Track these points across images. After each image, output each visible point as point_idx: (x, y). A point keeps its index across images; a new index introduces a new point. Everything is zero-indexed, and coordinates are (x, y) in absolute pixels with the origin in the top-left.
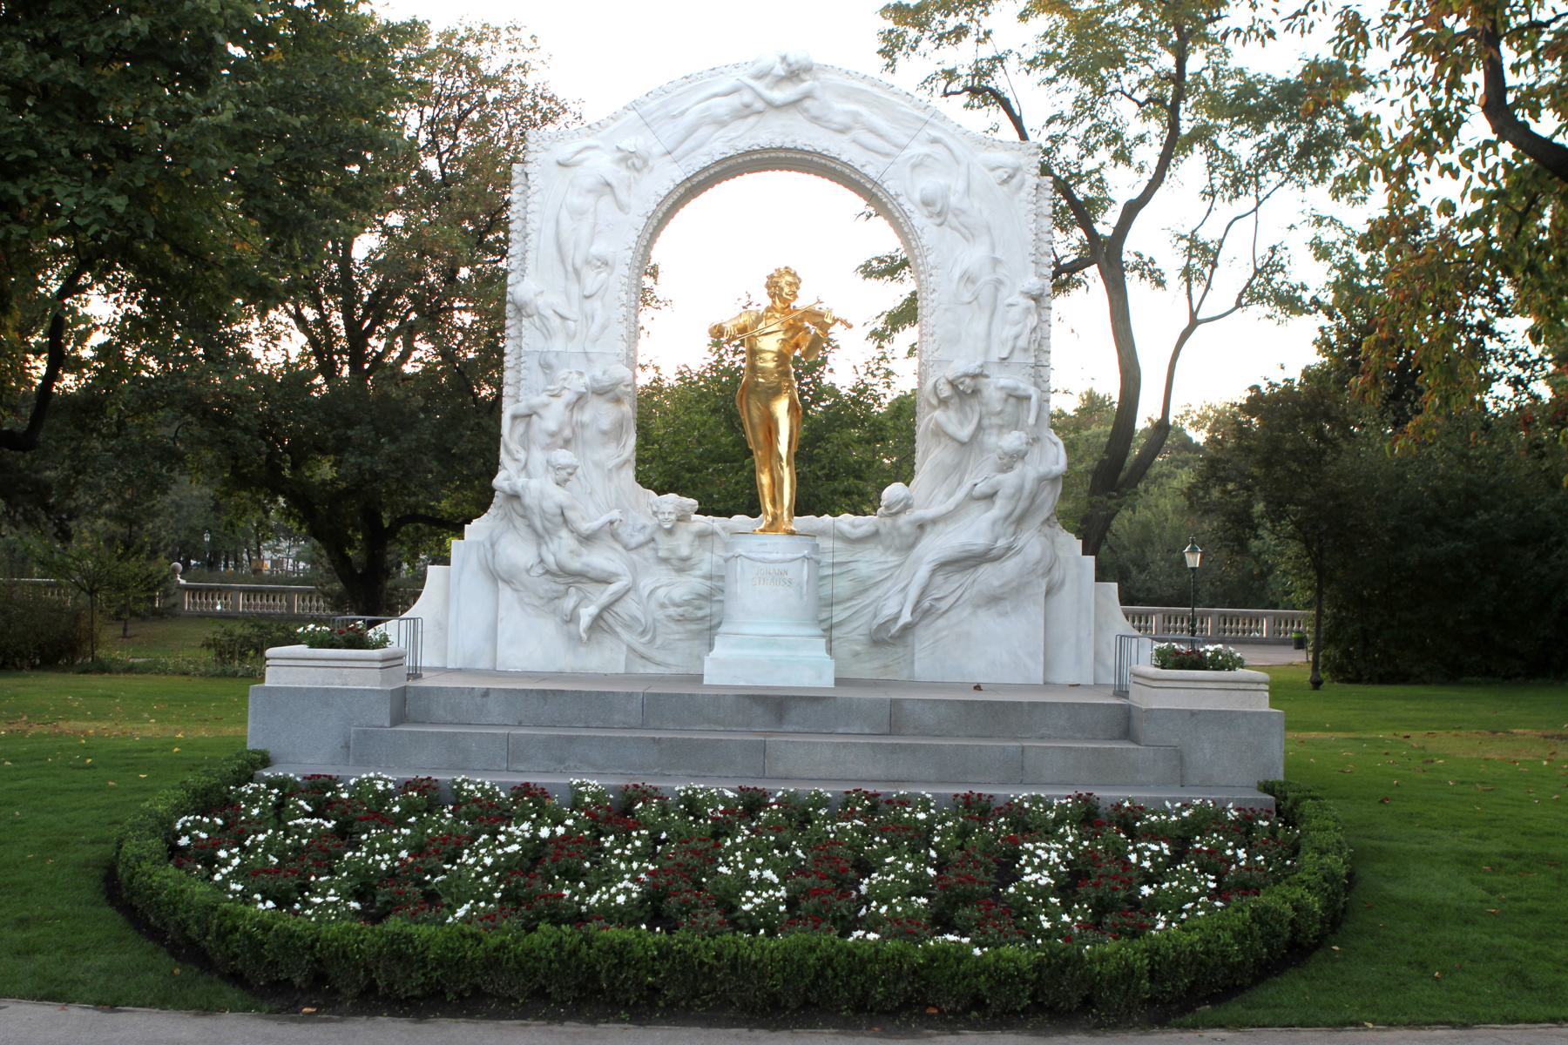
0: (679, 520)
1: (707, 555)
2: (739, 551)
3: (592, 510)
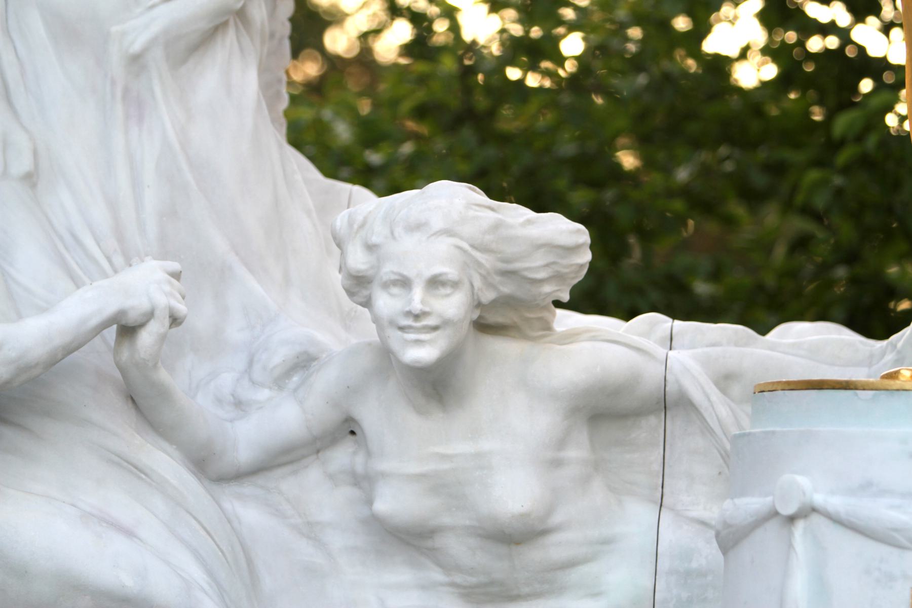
0: (486, 324)
1: (636, 519)
2: (806, 483)
3: (30, 262)
